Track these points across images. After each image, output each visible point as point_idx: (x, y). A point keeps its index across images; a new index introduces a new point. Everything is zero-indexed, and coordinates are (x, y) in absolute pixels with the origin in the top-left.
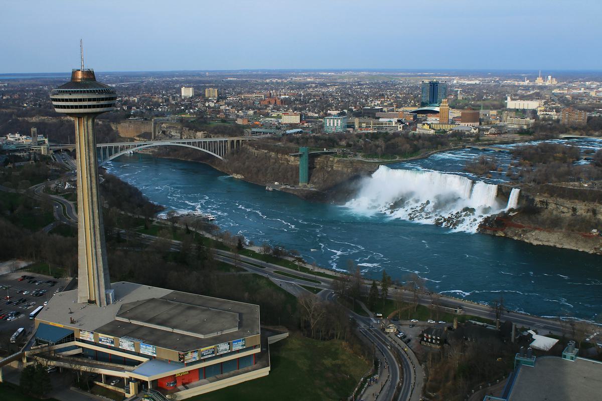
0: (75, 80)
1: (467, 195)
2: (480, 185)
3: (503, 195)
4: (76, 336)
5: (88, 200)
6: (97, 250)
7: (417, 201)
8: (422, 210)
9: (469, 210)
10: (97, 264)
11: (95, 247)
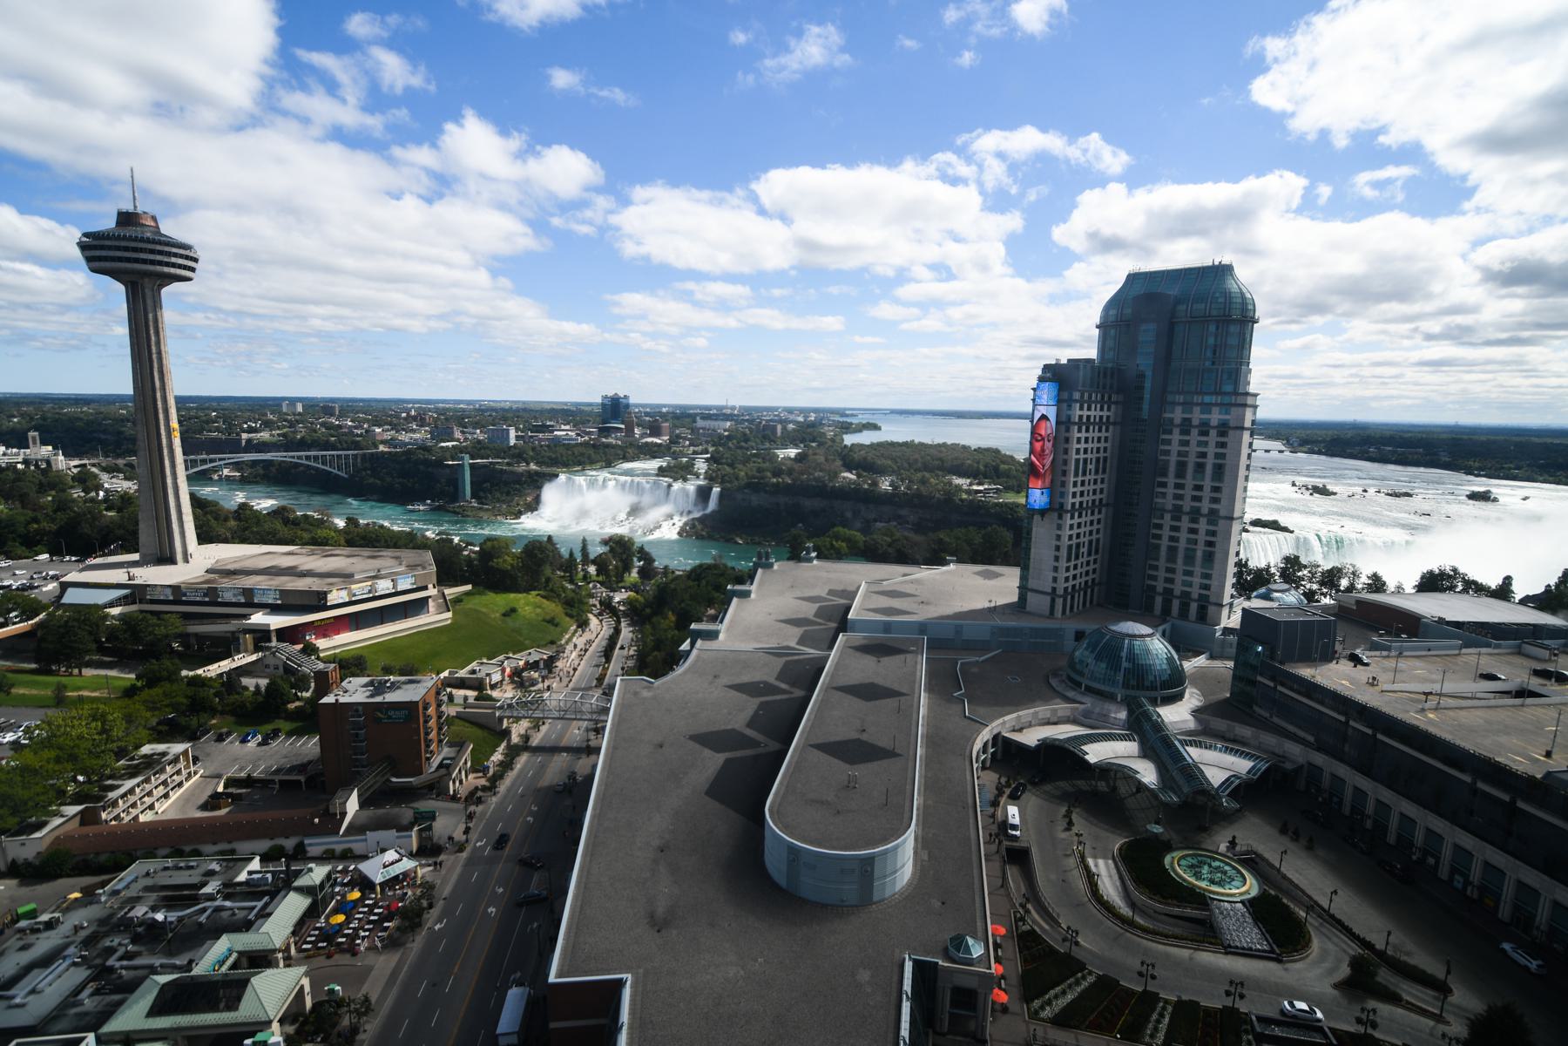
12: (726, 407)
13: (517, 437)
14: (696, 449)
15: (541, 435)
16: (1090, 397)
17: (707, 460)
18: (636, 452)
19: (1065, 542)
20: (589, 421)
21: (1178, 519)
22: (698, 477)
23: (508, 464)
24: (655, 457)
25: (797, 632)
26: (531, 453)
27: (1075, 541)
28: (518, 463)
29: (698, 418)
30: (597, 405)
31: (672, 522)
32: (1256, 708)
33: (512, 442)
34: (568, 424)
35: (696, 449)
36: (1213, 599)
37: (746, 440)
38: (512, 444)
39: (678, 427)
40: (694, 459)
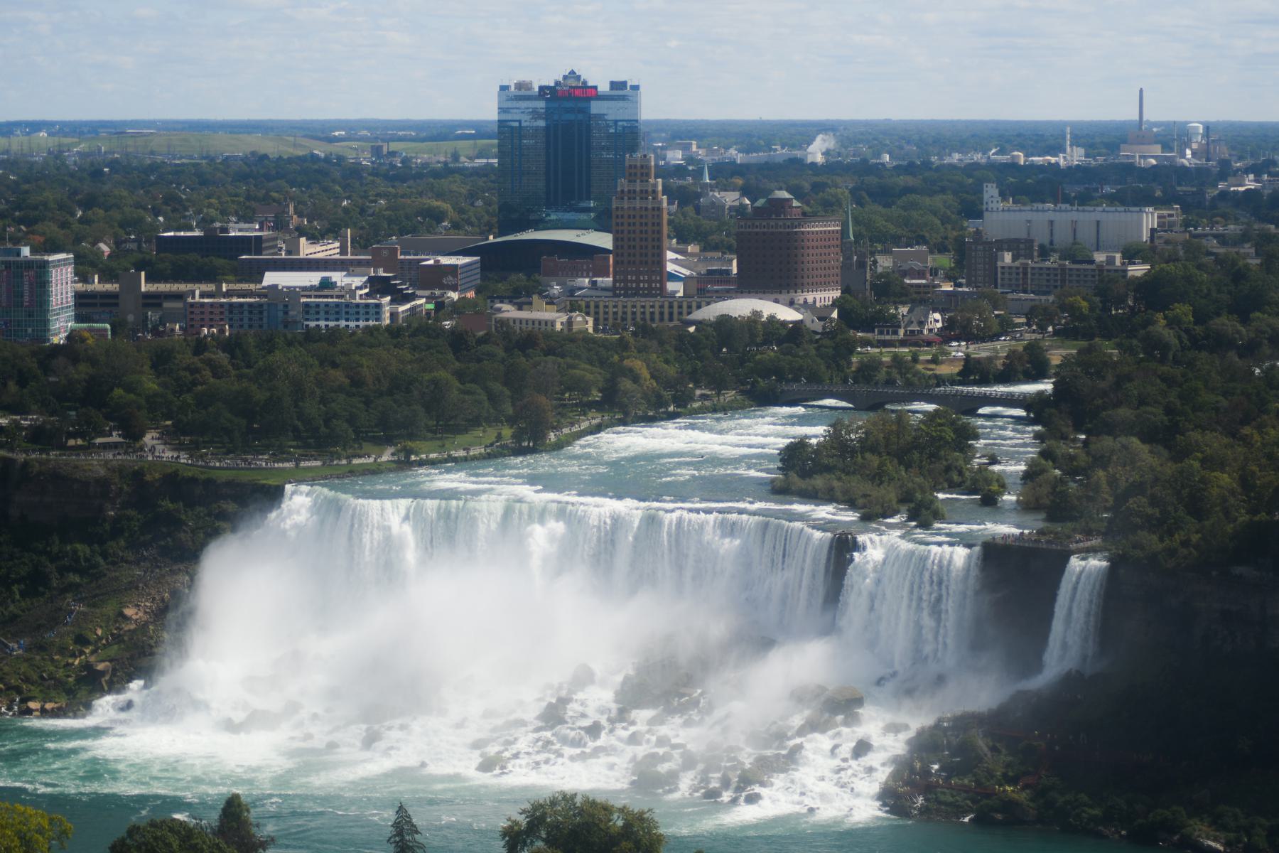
12: (1136, 133)
13: (85, 304)
14: (981, 351)
15: (198, 292)
17: (1036, 408)
18: (672, 371)
20: (438, 216)
22: (989, 501)
23: (38, 437)
24: (762, 398)
26: (150, 384)
28: (88, 430)
29: (991, 191)
30: (480, 131)
31: (849, 736)
33: (61, 326)
34: (331, 231)
35: (981, 351)
37: (1244, 308)
38: (58, 339)
39: (887, 241)
40: (971, 406)
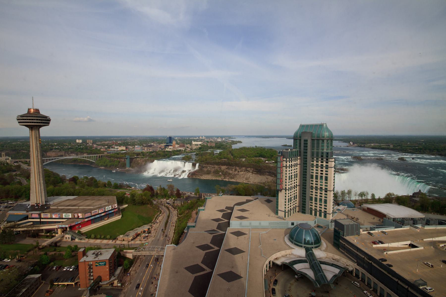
0: (30, 113)
1: (183, 166)
2: (187, 164)
3: (194, 165)
4: (29, 217)
5: (36, 161)
6: (41, 181)
7: (167, 170)
8: (170, 173)
9: (184, 171)
10: (40, 187)
11: (40, 180)
16: (292, 159)
19: (287, 198)
21: (317, 190)
25: (216, 224)
27: (290, 197)
32: (340, 241)
36: (327, 212)
